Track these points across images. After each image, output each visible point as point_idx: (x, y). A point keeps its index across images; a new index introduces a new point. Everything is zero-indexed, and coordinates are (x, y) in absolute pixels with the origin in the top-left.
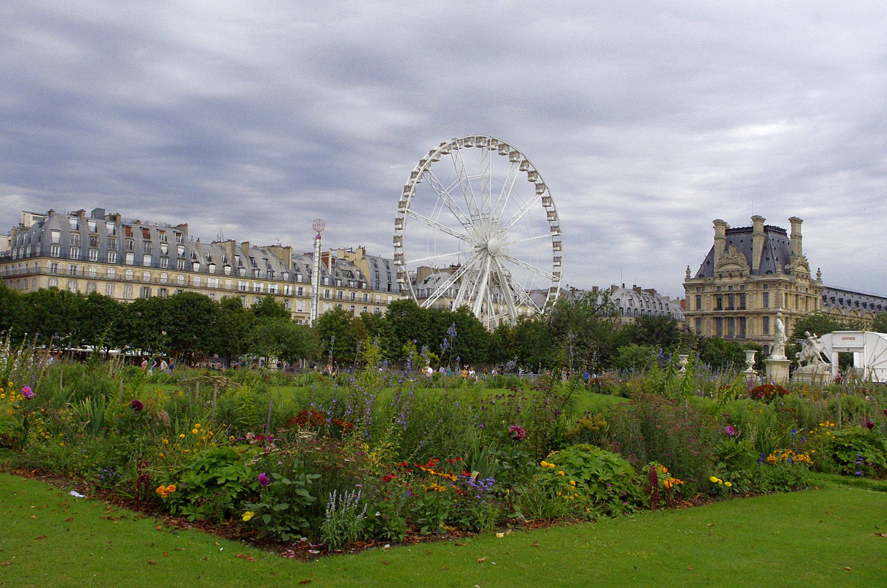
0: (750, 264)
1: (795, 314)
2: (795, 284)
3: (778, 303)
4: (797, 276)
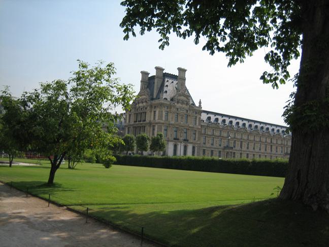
0: (152, 94)
1: (172, 124)
2: (174, 106)
3: (161, 117)
4: (178, 102)
